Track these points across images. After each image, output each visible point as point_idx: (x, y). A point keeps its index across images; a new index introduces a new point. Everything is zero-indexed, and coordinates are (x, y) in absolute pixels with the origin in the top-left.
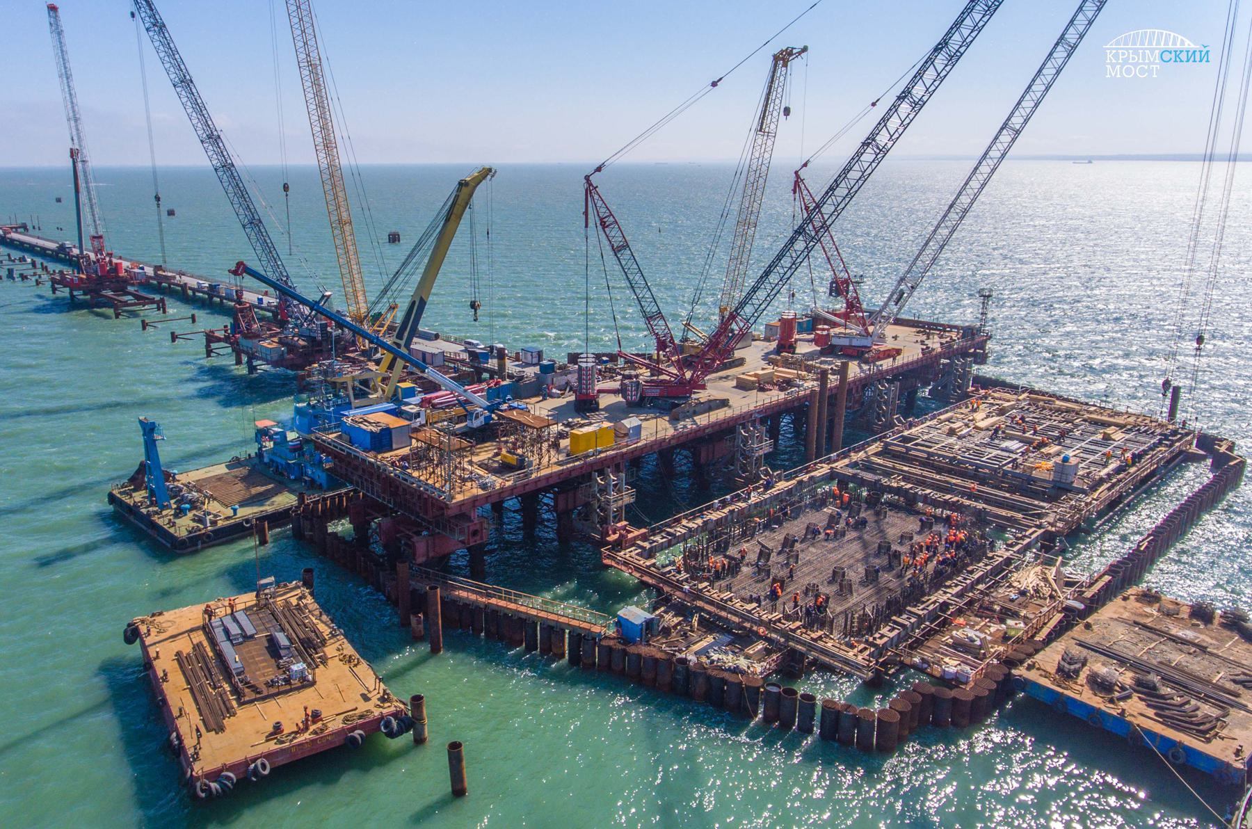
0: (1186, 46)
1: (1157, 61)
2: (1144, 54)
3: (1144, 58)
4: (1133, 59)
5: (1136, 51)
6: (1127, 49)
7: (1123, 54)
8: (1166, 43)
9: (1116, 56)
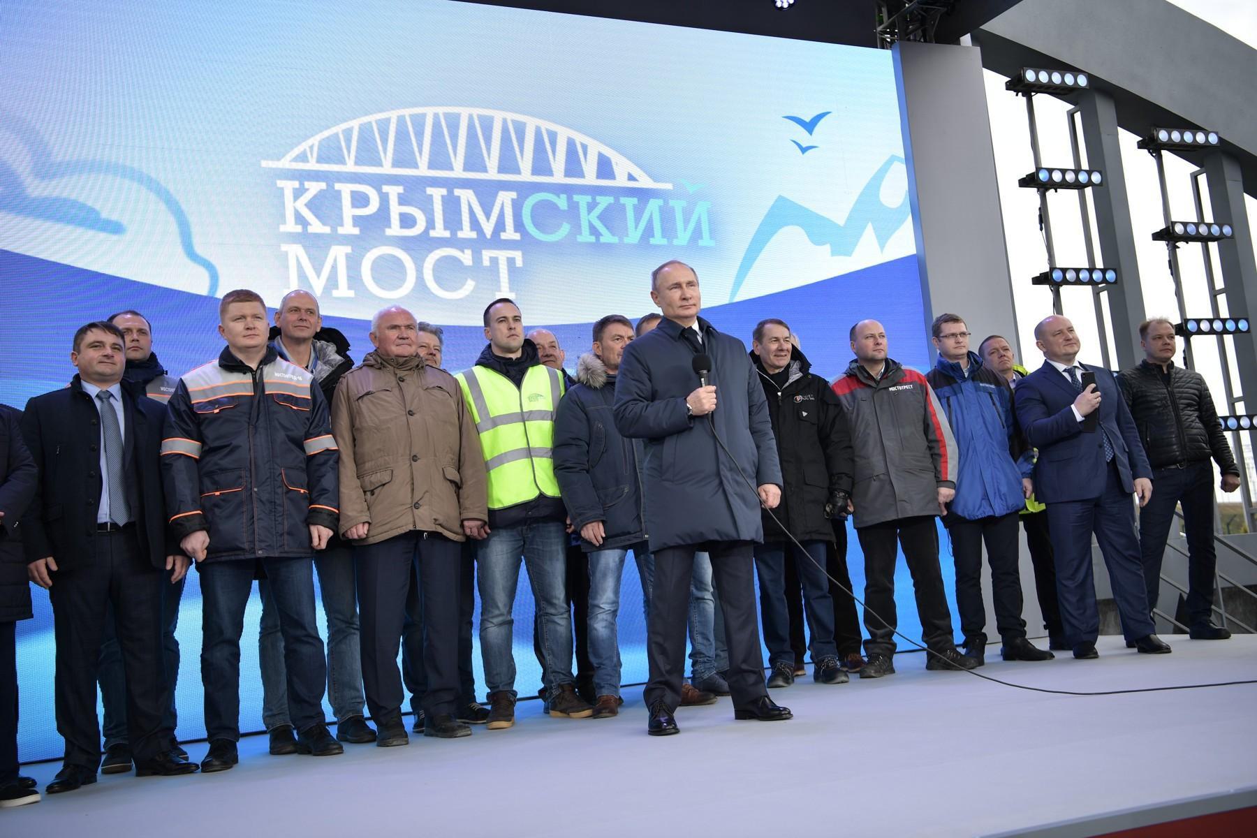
0: (621, 181)
1: (510, 234)
2: (451, 205)
3: (452, 220)
4: (407, 221)
5: (414, 190)
6: (378, 182)
7: (360, 200)
8: (541, 166)
9: (325, 206)
